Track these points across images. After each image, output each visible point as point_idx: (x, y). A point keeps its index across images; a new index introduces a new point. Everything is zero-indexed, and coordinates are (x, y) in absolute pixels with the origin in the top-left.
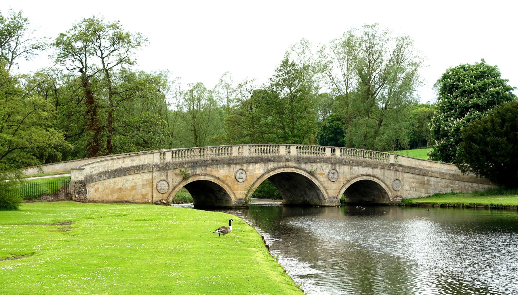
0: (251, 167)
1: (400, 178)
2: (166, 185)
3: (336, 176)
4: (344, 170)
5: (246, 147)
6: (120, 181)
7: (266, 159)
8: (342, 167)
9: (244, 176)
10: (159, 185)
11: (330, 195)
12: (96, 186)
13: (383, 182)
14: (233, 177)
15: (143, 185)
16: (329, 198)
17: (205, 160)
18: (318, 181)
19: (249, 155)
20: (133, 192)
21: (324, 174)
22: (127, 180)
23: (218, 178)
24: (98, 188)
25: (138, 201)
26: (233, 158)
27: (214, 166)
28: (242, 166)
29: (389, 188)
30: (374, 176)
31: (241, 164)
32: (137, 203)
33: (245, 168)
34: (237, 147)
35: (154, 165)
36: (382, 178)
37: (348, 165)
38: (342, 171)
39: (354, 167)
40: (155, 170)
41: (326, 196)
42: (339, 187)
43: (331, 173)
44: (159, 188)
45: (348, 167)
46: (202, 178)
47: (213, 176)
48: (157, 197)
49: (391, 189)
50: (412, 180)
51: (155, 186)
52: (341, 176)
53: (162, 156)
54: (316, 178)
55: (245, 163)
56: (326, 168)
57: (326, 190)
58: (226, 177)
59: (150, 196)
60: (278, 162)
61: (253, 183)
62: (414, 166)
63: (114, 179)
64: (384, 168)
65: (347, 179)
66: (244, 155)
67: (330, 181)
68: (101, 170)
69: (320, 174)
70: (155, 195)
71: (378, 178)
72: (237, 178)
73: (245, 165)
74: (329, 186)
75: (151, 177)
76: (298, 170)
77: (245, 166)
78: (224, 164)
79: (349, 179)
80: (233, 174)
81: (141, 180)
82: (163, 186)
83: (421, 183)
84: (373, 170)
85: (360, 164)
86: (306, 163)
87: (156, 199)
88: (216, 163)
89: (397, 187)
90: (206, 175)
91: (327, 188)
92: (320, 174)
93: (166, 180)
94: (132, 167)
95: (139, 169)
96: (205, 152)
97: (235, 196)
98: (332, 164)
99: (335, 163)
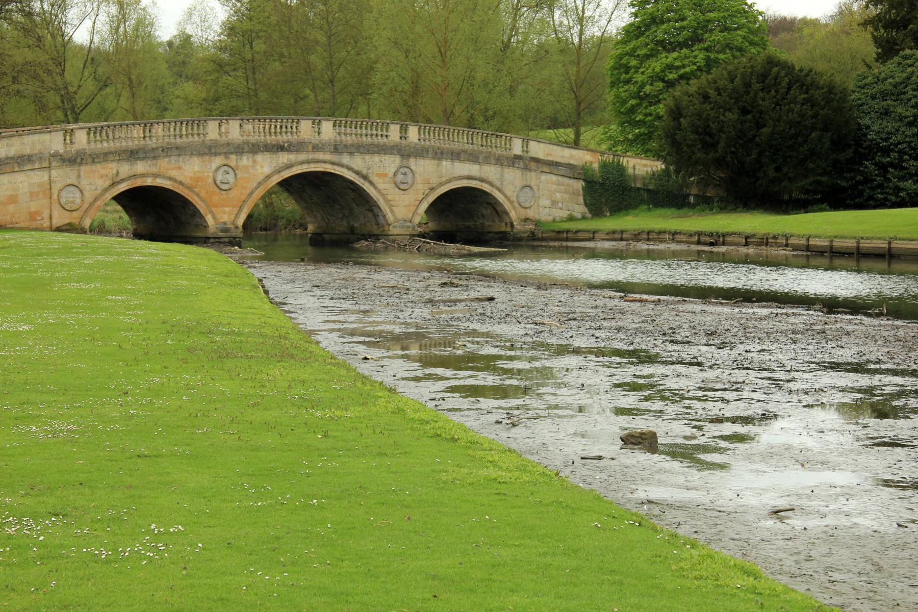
0: (245, 160)
1: (533, 184)
2: (78, 194)
3: (409, 180)
5: (234, 121)
7: (274, 146)
9: (231, 178)
10: (64, 194)
13: (499, 190)
14: (210, 180)
15: (32, 194)
16: (397, 220)
17: (154, 146)
19: (240, 137)
20: (11, 208)
21: (386, 175)
23: (181, 183)
25: (22, 225)
26: (208, 143)
27: (173, 158)
29: (511, 202)
30: (482, 180)
31: (226, 155)
32: (21, 229)
33: (233, 164)
34: (217, 123)
36: (498, 184)
37: (434, 158)
38: (422, 169)
39: (444, 163)
40: (54, 164)
42: (416, 200)
43: (399, 173)
44: (63, 201)
46: (149, 182)
47: (170, 179)
48: (60, 218)
49: (516, 204)
50: (555, 186)
51: (55, 196)
52: (418, 178)
53: (68, 138)
54: (371, 183)
55: (232, 153)
56: (391, 163)
57: (391, 206)
58: (197, 179)
59: (46, 215)
61: (248, 191)
62: (558, 160)
64: (502, 165)
65: (430, 186)
66: (230, 137)
67: (397, 189)
69: (379, 175)
70: (56, 214)
71: (491, 184)
72: (218, 183)
73: (233, 157)
75: (46, 178)
76: (336, 167)
78: (192, 154)
79: (434, 185)
80: (211, 175)
81: (26, 184)
83: (574, 193)
84: (481, 169)
85: (455, 156)
86: (351, 153)
87: (57, 222)
88: (177, 152)
89: (526, 201)
90: (155, 176)
91: (392, 203)
92: (379, 175)
93: (76, 184)
94: (7, 158)
96: (153, 131)
97: (214, 217)
98: (402, 156)
99: (406, 153)
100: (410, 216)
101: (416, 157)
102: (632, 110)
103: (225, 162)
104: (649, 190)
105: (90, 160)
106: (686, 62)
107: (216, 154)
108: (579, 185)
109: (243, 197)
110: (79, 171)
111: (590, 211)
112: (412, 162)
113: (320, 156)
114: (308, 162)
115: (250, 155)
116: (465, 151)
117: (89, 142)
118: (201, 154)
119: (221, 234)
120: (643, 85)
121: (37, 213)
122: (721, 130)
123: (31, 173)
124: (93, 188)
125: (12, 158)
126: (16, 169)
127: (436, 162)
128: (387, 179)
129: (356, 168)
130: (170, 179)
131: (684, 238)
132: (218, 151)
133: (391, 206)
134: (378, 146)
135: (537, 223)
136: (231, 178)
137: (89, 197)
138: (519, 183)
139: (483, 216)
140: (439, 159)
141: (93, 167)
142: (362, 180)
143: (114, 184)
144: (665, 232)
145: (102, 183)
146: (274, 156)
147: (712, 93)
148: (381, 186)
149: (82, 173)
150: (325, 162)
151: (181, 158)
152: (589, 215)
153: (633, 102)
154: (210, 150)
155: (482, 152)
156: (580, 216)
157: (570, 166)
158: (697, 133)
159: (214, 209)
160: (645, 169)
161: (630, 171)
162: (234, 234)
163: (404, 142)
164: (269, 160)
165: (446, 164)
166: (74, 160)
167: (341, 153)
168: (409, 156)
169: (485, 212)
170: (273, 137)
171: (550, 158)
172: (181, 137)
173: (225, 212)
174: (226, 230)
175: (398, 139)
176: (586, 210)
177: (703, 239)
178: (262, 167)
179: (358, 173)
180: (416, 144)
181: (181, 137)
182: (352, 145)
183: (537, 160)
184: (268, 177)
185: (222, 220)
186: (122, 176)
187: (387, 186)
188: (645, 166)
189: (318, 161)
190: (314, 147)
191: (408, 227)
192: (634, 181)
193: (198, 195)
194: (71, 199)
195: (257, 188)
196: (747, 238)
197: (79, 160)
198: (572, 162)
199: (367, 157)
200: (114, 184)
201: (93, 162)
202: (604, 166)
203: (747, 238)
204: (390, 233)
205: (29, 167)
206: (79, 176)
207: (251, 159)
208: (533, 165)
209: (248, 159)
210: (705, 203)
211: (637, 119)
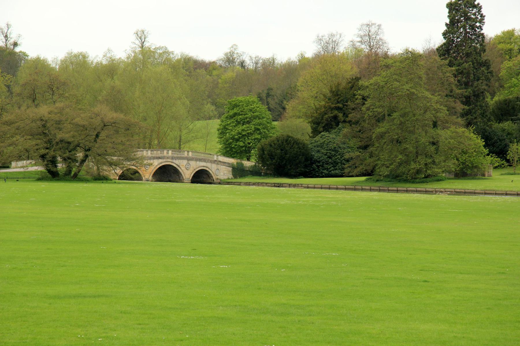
1: (219, 168)
13: (211, 170)
18: (181, 169)
21: (183, 165)
28: (148, 161)
29: (214, 174)
30: (207, 167)
36: (210, 168)
37: (195, 161)
41: (184, 177)
50: (224, 169)
54: (180, 168)
56: (185, 162)
57: (184, 175)
60: (164, 159)
61: (152, 170)
62: (226, 162)
64: (212, 163)
71: (209, 169)
73: (149, 160)
83: (229, 171)
86: (176, 159)
99: (189, 159)
100: (189, 177)
102: (231, 143)
104: (250, 171)
106: (248, 129)
108: (231, 169)
109: (151, 172)
111: (234, 177)
112: (190, 162)
114: (166, 162)
120: (235, 135)
122: (276, 155)
131: (270, 185)
133: (184, 175)
134: (182, 157)
135: (221, 180)
138: (216, 168)
139: (204, 177)
140: (197, 161)
144: (263, 183)
147: (273, 144)
148: (182, 169)
150: (169, 162)
152: (233, 178)
153: (231, 141)
155: (207, 159)
156: (231, 178)
157: (228, 163)
158: (269, 156)
160: (249, 164)
161: (245, 165)
165: (198, 162)
168: (189, 160)
169: (204, 176)
171: (223, 161)
175: (186, 155)
176: (232, 176)
177: (276, 185)
179: (177, 165)
183: (220, 161)
188: (249, 163)
189: (168, 162)
192: (246, 168)
196: (289, 185)
198: (229, 162)
199: (180, 161)
202: (237, 163)
203: (289, 185)
208: (219, 163)
210: (266, 175)
211: (232, 146)
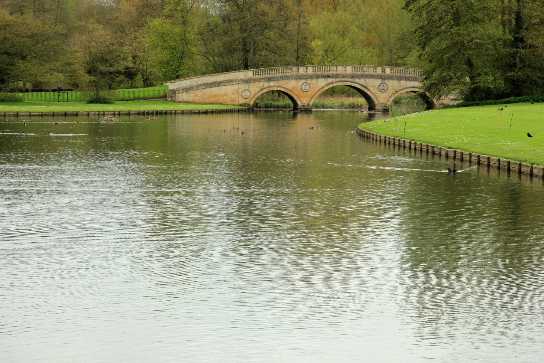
0: (314, 81)
2: (249, 93)
3: (386, 88)
4: (393, 84)
5: (301, 68)
6: (216, 90)
7: (326, 76)
8: (391, 81)
9: (308, 87)
11: (380, 102)
12: (196, 93)
14: (299, 88)
17: (278, 76)
18: (370, 91)
20: (225, 97)
21: (375, 86)
22: (221, 90)
23: (288, 89)
24: (197, 94)
25: (229, 103)
27: (285, 80)
31: (306, 79)
35: (240, 80)
37: (397, 80)
39: (402, 82)
40: (240, 83)
41: (376, 102)
42: (388, 96)
44: (243, 95)
45: (396, 81)
47: (283, 88)
51: (240, 94)
52: (390, 88)
54: (368, 89)
55: (308, 79)
56: (378, 82)
58: (294, 88)
59: (237, 100)
61: (315, 92)
63: (211, 89)
65: (395, 90)
67: (380, 92)
68: (200, 83)
70: (240, 99)
72: (303, 89)
73: (309, 80)
74: (380, 95)
75: (238, 87)
77: (309, 81)
78: (292, 79)
79: (397, 90)
80: (300, 86)
82: (247, 94)
85: (407, 79)
86: (359, 78)
88: (286, 78)
91: (377, 97)
93: (248, 89)
94: (224, 81)
95: (229, 82)
98: (382, 79)
99: (383, 78)
100: (386, 102)
101: (388, 79)
103: (306, 82)
105: (253, 81)
107: (302, 79)
109: (313, 94)
110: (249, 85)
112: (387, 81)
113: (346, 79)
114: (340, 82)
115: (316, 79)
116: (412, 77)
117: (253, 75)
118: (296, 79)
119: (302, 108)
121: (234, 99)
123: (232, 86)
124: (254, 91)
125: (226, 81)
126: (227, 84)
127: (398, 81)
128: (375, 88)
129: (361, 84)
130: (283, 88)
132: (303, 78)
136: (308, 87)
137: (253, 94)
140: (399, 80)
141: (254, 84)
142: (364, 88)
143: (262, 89)
145: (257, 89)
146: (326, 79)
148: (373, 90)
149: (250, 86)
150: (347, 81)
151: (288, 80)
154: (299, 77)
159: (301, 99)
162: (306, 108)
163: (383, 73)
164: (323, 81)
165: (403, 82)
166: (247, 81)
167: (355, 78)
168: (385, 79)
170: (326, 72)
172: (316, 71)
173: (305, 100)
174: (303, 106)
178: (321, 83)
179: (362, 85)
180: (389, 74)
181: (265, 75)
182: (360, 75)
184: (323, 87)
185: (304, 103)
186: (265, 87)
187: (375, 90)
189: (344, 81)
190: (343, 76)
191: (382, 106)
193: (294, 93)
194: (246, 95)
195: (318, 91)
197: (249, 81)
200: (262, 89)
201: (254, 82)
204: (376, 108)
205: (232, 84)
206: (249, 87)
207: (316, 81)
209: (315, 81)
